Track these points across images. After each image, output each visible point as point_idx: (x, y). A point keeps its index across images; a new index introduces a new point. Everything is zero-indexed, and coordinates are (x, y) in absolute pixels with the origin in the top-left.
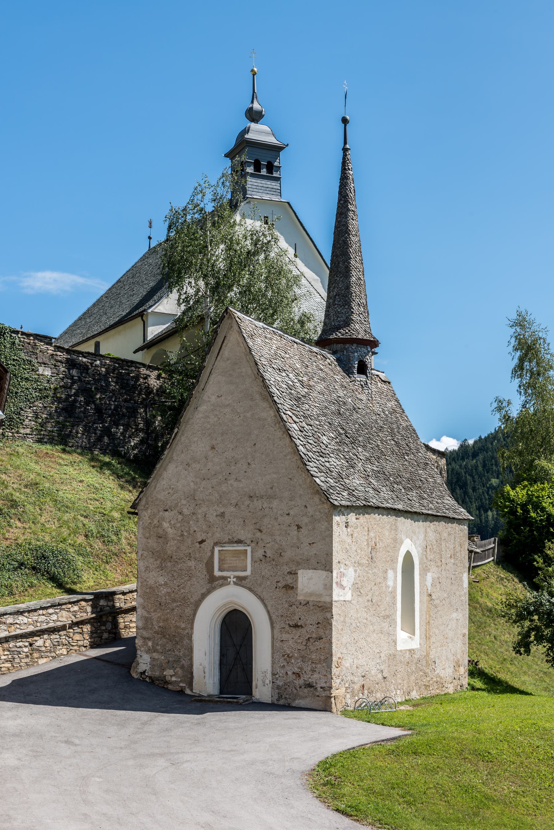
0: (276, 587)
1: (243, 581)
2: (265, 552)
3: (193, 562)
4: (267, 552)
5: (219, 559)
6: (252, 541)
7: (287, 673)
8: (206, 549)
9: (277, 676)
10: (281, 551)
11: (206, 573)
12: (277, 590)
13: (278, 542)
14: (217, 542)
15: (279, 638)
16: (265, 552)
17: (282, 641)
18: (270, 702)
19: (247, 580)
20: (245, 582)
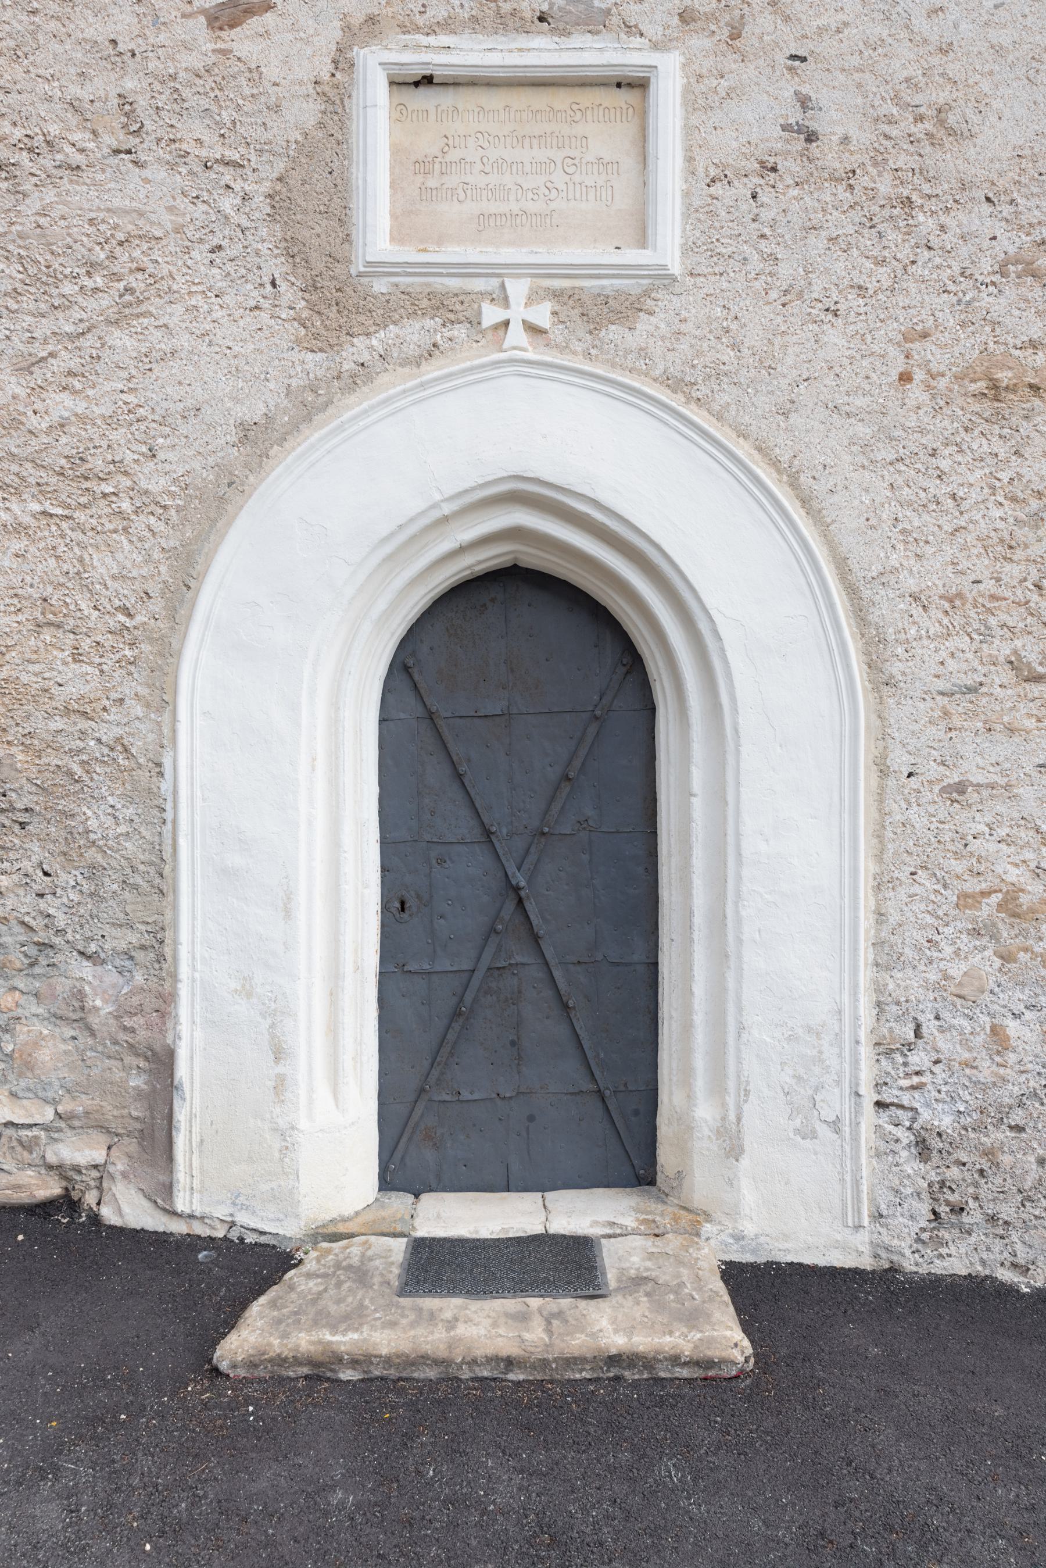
0: (905, 378)
1: (614, 333)
2: (804, 102)
3: (157, 173)
4: (821, 96)
5: (396, 150)
6: (686, 17)
7: (996, 1031)
8: (272, 72)
9: (919, 1058)
10: (942, 97)
11: (276, 267)
12: (916, 393)
13: (921, 24)
14: (371, 20)
15: (934, 770)
16: (804, 102)
17: (960, 788)
18: (866, 1263)
19: (644, 324)
20: (633, 340)
